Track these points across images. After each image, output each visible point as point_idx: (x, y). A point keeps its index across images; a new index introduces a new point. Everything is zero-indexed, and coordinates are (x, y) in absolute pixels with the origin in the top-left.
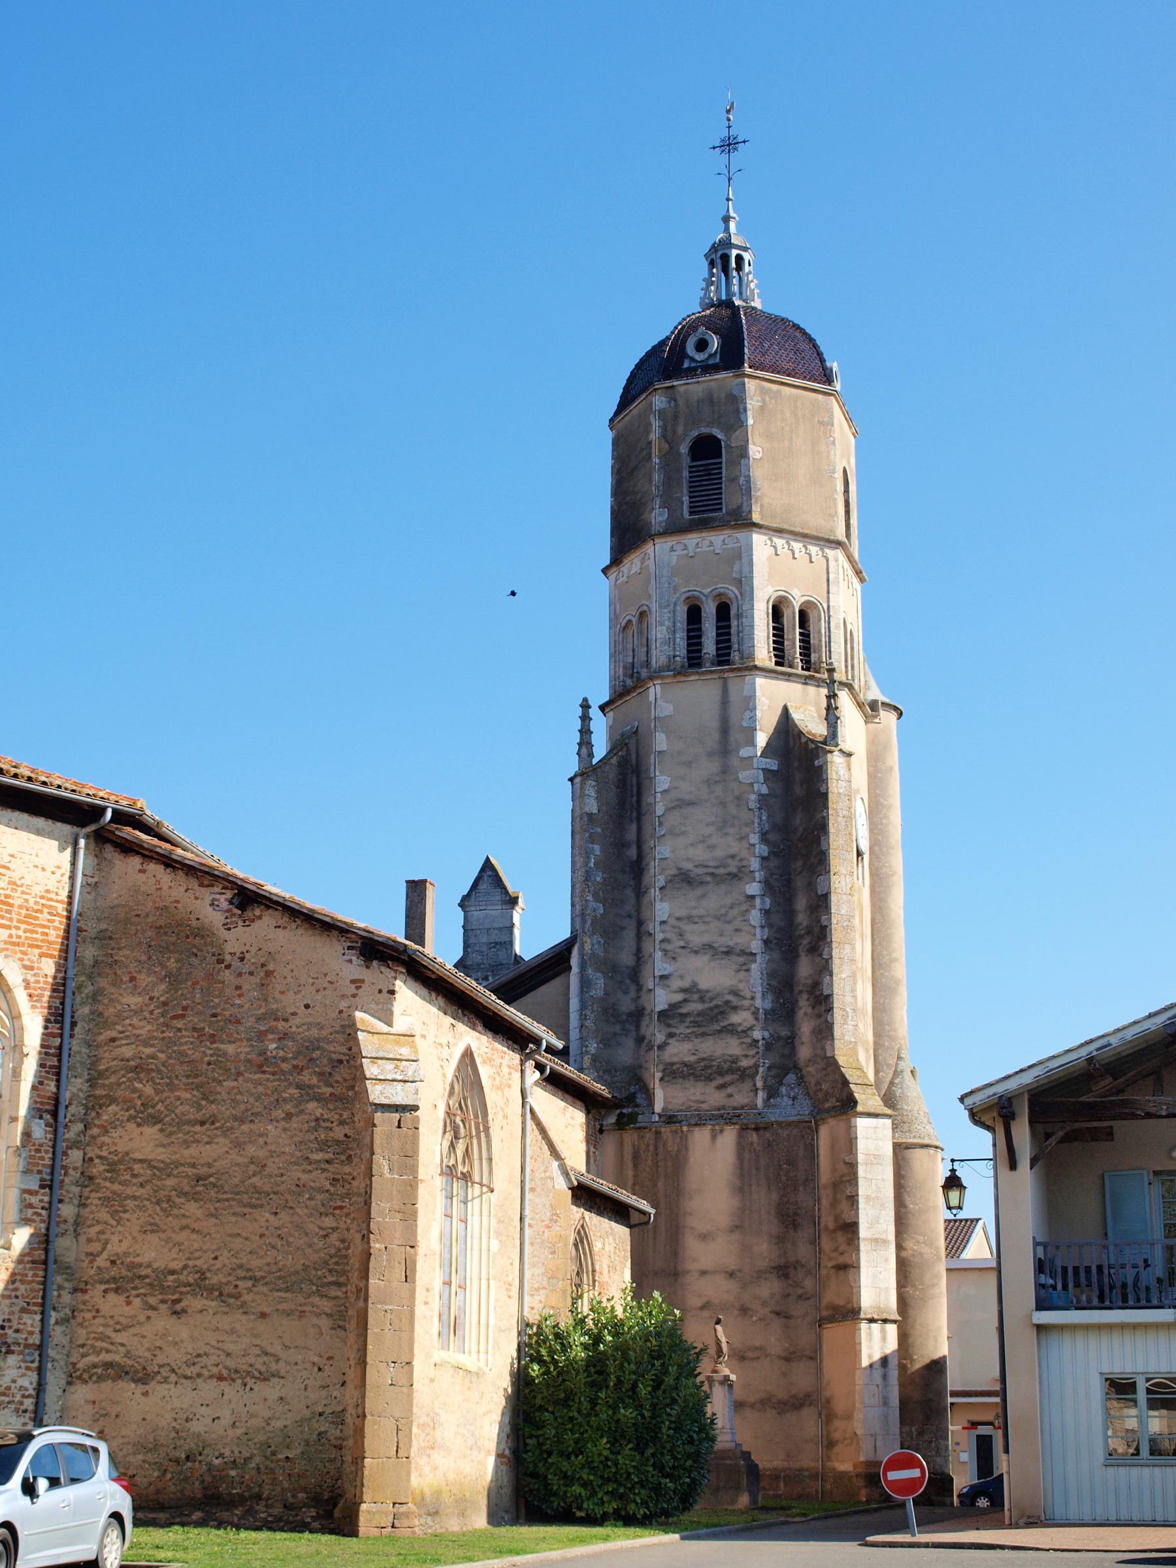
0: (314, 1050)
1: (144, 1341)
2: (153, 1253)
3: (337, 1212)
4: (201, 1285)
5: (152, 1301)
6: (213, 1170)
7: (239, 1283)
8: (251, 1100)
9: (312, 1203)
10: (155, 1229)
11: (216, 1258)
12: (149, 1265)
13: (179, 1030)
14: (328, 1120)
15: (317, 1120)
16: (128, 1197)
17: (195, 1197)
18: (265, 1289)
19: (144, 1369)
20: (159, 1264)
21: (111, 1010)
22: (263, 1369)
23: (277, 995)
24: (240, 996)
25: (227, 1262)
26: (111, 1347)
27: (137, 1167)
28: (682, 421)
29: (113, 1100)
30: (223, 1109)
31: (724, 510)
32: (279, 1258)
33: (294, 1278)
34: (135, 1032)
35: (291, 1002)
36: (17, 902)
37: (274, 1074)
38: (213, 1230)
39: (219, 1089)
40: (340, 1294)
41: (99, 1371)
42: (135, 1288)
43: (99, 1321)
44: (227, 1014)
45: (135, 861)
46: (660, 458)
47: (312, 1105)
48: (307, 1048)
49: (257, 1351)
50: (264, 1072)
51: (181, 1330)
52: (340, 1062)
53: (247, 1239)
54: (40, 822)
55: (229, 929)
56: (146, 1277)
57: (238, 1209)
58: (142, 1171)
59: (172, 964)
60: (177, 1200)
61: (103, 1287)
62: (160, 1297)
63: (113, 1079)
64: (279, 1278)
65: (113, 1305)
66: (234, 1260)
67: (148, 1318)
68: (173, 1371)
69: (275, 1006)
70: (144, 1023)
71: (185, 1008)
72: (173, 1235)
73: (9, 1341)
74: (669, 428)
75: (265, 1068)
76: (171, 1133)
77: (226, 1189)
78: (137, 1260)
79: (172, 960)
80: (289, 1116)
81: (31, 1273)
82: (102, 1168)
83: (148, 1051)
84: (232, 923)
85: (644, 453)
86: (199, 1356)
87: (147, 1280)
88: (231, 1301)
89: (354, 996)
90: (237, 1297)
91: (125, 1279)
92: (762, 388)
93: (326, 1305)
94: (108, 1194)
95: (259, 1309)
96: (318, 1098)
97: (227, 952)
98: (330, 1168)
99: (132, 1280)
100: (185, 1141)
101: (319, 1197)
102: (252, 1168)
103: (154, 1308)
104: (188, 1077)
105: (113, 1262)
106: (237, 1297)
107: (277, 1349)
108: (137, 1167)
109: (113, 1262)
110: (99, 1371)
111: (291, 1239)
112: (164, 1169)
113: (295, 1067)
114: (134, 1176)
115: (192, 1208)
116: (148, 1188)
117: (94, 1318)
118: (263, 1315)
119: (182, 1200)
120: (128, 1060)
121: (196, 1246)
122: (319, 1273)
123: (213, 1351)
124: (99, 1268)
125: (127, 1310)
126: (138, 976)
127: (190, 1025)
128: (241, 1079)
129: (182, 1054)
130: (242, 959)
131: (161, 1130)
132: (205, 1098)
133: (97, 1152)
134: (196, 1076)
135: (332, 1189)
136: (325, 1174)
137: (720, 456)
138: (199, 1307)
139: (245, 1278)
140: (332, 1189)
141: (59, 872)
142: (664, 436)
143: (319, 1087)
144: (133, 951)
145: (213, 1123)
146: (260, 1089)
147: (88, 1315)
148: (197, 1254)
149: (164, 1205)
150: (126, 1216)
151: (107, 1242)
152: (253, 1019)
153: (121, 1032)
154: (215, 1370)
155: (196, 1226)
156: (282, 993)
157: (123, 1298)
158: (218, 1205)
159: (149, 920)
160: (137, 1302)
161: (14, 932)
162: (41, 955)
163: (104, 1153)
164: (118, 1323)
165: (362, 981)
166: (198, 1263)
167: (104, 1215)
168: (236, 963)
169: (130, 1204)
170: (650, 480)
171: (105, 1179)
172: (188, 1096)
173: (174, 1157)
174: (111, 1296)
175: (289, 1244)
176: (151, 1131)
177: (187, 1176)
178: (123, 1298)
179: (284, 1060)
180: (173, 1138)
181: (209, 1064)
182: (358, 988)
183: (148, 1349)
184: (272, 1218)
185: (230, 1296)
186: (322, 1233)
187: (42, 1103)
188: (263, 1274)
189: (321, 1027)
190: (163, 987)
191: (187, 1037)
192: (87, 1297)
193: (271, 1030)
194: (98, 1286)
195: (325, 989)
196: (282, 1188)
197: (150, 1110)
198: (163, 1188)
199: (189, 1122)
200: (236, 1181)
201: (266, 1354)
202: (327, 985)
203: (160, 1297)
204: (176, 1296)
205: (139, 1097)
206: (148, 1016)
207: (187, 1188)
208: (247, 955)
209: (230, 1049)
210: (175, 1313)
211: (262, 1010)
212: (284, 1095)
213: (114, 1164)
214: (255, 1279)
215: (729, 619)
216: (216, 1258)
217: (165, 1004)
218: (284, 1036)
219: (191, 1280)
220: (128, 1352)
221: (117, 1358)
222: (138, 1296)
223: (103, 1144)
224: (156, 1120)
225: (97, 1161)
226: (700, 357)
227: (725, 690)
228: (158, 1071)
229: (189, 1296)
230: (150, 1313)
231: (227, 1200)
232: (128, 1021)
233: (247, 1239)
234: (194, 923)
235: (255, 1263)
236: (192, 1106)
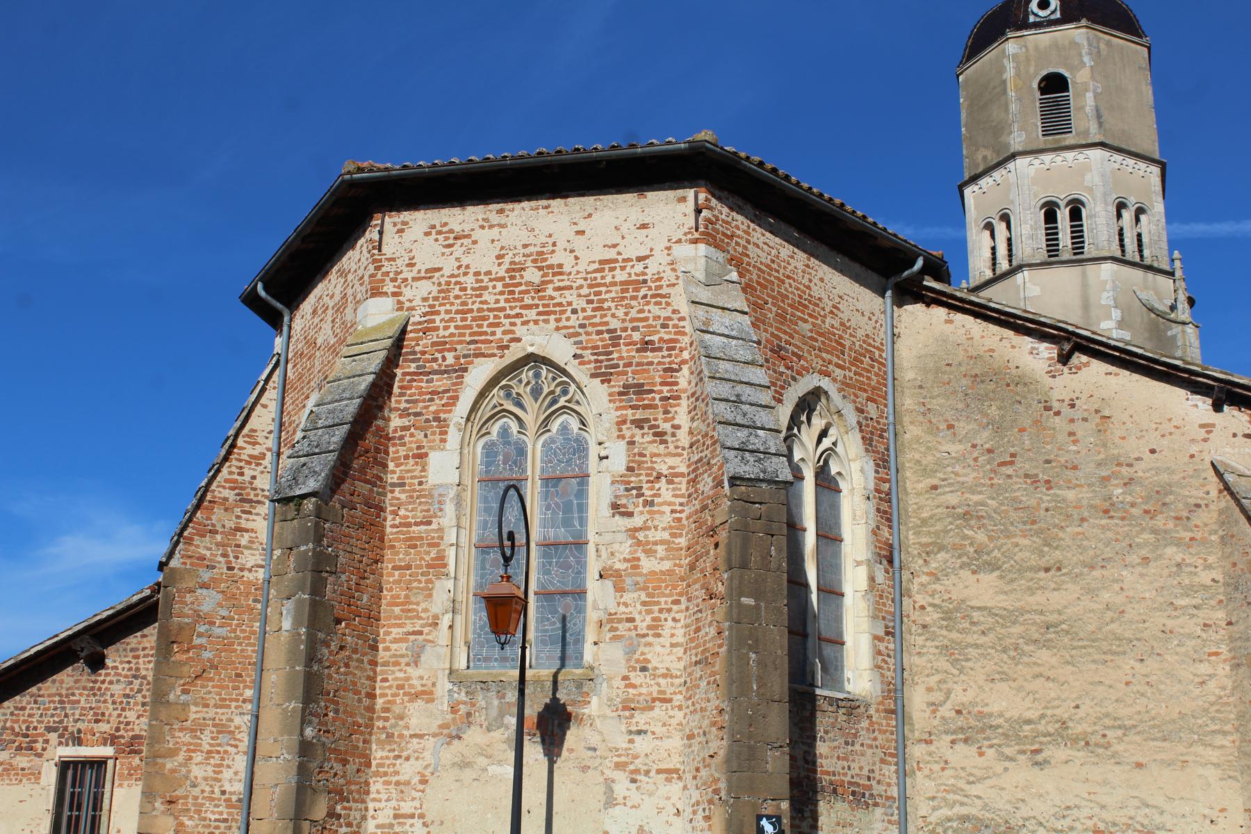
0: (1166, 494)
1: (1003, 793)
2: (1003, 702)
3: (1213, 658)
4: (1062, 733)
5: (1008, 751)
6: (1063, 617)
7: (1107, 732)
8: (1100, 545)
9: (1182, 650)
10: (1005, 677)
11: (1077, 707)
12: (1001, 715)
13: (1009, 476)
14: (1190, 565)
15: (1178, 565)
16: (968, 645)
17: (1048, 644)
18: (1138, 738)
19: (1007, 822)
20: (1013, 713)
21: (930, 458)
22: (1146, 822)
23: (1117, 440)
24: (1075, 442)
25: (1091, 711)
26: (966, 800)
27: (976, 615)
28: (1033, 63)
29: (942, 548)
30: (1069, 555)
32: (1150, 706)
33: (1170, 727)
34: (961, 479)
35: (1134, 447)
36: (847, 343)
37: (1123, 519)
38: (1071, 679)
39: (1061, 535)
40: (1228, 744)
41: (955, 824)
42: (988, 739)
43: (947, 772)
44: (1062, 460)
45: (940, 312)
47: (1170, 551)
48: (1158, 492)
49: (1136, 803)
50: (1112, 517)
51: (1042, 780)
52: (1198, 506)
53: (1111, 687)
54: (856, 267)
55: (1054, 377)
56: (999, 727)
57: (1096, 657)
58: (982, 619)
59: (993, 411)
60: (1026, 648)
61: (950, 738)
62: (1017, 748)
63: (939, 527)
64: (1154, 727)
65: (962, 755)
66: (1098, 709)
67: (1006, 769)
68: (1041, 824)
69: (1116, 452)
70: (968, 470)
71: (1013, 455)
72: (1025, 684)
73: (875, 792)
75: (1112, 513)
76: (1012, 580)
77: (1081, 635)
78: (986, 710)
79: (994, 408)
80: (1146, 560)
81: (884, 722)
82: (936, 616)
83: (976, 498)
84: (1056, 371)
86: (1068, 808)
87: (1000, 730)
88: (1100, 751)
89: (1205, 440)
90: (1107, 746)
91: (973, 729)
93: (1212, 755)
94: (946, 642)
95: (1134, 759)
96: (1178, 543)
97: (1054, 399)
98: (1200, 613)
99: (982, 730)
100: (1029, 588)
101: (1191, 643)
102: (1109, 614)
103: (1011, 759)
104: (1024, 523)
105: (959, 712)
106: (1107, 746)
107: (1159, 800)
108: (976, 615)
109: (959, 712)
110: (955, 824)
111: (1162, 687)
112: (1011, 617)
113: (1146, 512)
114: (973, 623)
115: (1044, 655)
116: (991, 636)
117: (943, 769)
118: (1139, 765)
119: (1032, 648)
120: (953, 508)
121: (1053, 695)
122: (1200, 721)
123: (1084, 803)
124: (943, 718)
125: (981, 761)
126: (956, 424)
127: (1021, 472)
128: (1085, 524)
129: (1014, 499)
130: (1073, 406)
131: (1001, 577)
132: (1049, 545)
133: (930, 600)
134: (1034, 522)
135: (1204, 635)
136: (1194, 620)
138: (1064, 758)
139: (1113, 727)
140: (1204, 635)
141: (874, 318)
142: (1018, 75)
143: (1177, 532)
144: (947, 400)
145: (1059, 569)
146: (1109, 534)
147: (936, 767)
148: (1056, 703)
149: (1012, 653)
150: (970, 664)
151: (949, 692)
152: (1093, 465)
153: (943, 480)
154: (1090, 823)
155: (1049, 674)
156: (1123, 438)
157: (973, 750)
158: (1074, 652)
159: (963, 369)
160: (990, 753)
161: (847, 373)
162: (869, 399)
163: (937, 601)
164: (971, 774)
165: (1213, 425)
166: (1057, 712)
167: (943, 664)
168: (1065, 410)
169: (972, 652)
171: (941, 627)
172: (1026, 542)
173: (1018, 604)
174: (960, 747)
175: (1161, 692)
176: (989, 579)
177: (1035, 623)
178: (973, 750)
179: (1133, 505)
180: (1015, 585)
181: (1047, 510)
182: (1209, 432)
183: (1009, 802)
184: (1138, 665)
185: (1097, 745)
186: (1197, 680)
187: (880, 548)
188: (1132, 722)
189: (1171, 472)
190: (986, 434)
191: (1018, 483)
192: (932, 748)
193: (1115, 475)
194: (944, 736)
195: (1171, 434)
196: (1146, 634)
197: (985, 557)
198: (1009, 635)
199: (1031, 569)
200: (1091, 628)
201: (1148, 806)
202: (1173, 430)
203: (1017, 748)
204: (1036, 747)
205: (971, 544)
206: (972, 463)
207: (1036, 636)
208: (1077, 402)
209: (1071, 495)
210: (1036, 763)
211: (1102, 456)
212: (1137, 540)
213: (949, 612)
214: (1126, 729)
215: (1080, 219)
216: (1077, 707)
217: (990, 451)
218: (1129, 482)
219: (1051, 730)
220: (986, 805)
221: (974, 811)
222: (991, 746)
223: (934, 591)
224: (993, 566)
225: (929, 609)
226: (1042, 13)
227: (1084, 274)
228: (990, 517)
229: (1051, 746)
230: (1007, 764)
231: (1084, 647)
232: (949, 469)
233: (1111, 687)
234: (1014, 371)
235: (1123, 712)
236: (1033, 552)
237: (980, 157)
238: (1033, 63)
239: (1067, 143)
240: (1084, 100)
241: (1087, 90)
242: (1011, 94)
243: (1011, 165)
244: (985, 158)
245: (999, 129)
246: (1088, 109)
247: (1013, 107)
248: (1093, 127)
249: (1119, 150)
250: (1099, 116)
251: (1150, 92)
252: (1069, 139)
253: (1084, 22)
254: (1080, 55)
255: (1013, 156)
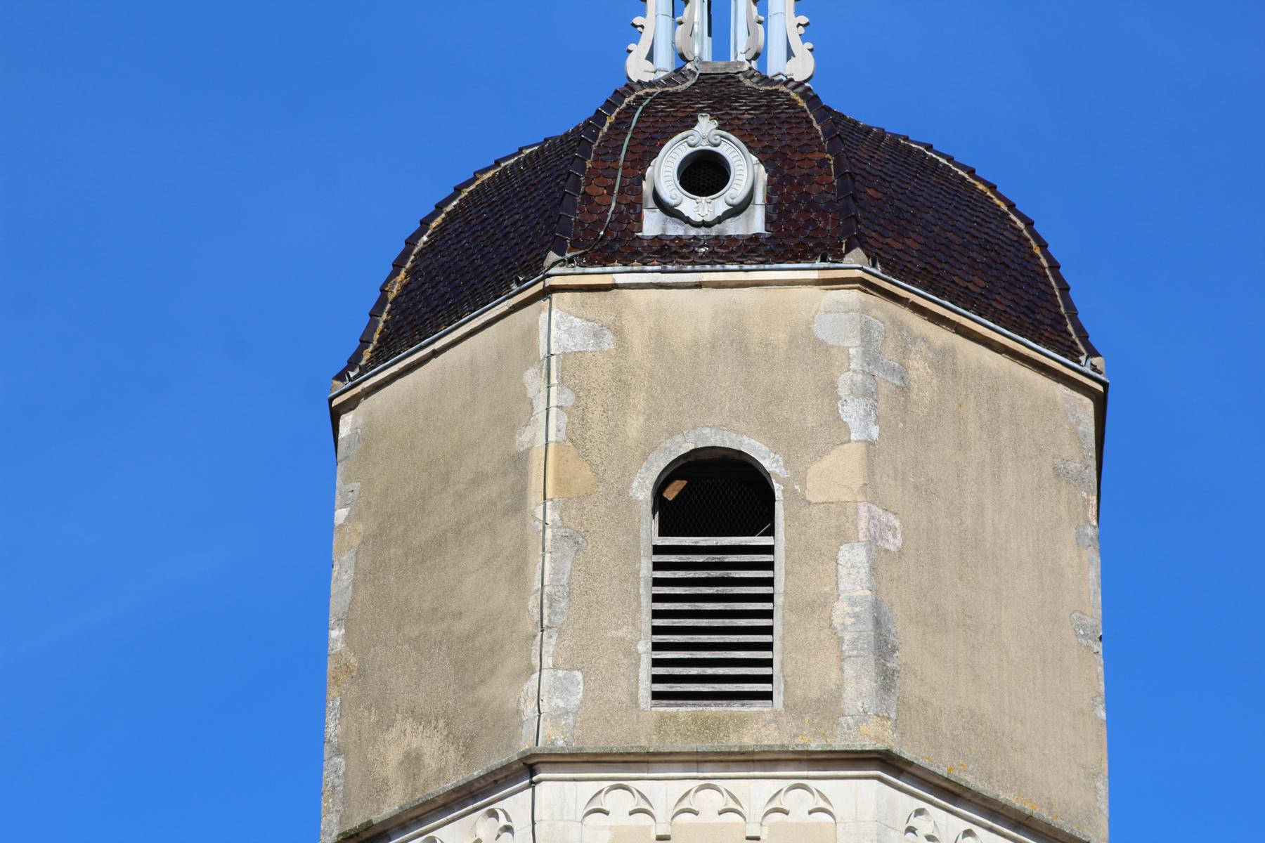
28: (640, 399)
31: (778, 698)
46: (563, 510)
74: (595, 414)
85: (494, 489)
92: (900, 326)
137: (771, 532)
142: (576, 439)
170: (519, 573)
226: (697, 208)
237: (394, 756)
238: (640, 399)
239: (748, 739)
240: (827, 576)
241: (842, 536)
242: (544, 512)
243: (515, 804)
244: (413, 761)
245: (478, 654)
246: (841, 612)
247: (549, 568)
248: (858, 687)
249: (951, 793)
250: (883, 647)
251: (1093, 574)
252: (756, 725)
253: (855, 262)
254: (829, 391)
255: (527, 768)
